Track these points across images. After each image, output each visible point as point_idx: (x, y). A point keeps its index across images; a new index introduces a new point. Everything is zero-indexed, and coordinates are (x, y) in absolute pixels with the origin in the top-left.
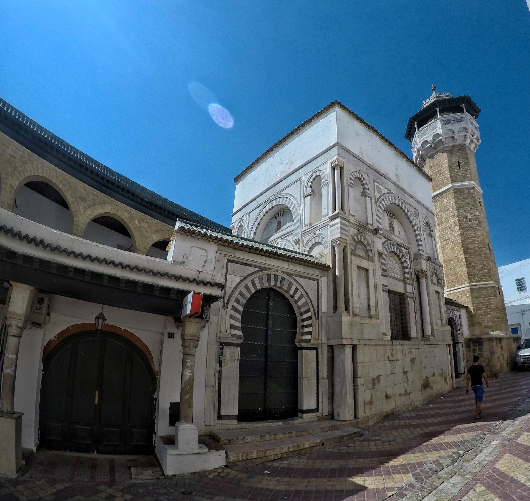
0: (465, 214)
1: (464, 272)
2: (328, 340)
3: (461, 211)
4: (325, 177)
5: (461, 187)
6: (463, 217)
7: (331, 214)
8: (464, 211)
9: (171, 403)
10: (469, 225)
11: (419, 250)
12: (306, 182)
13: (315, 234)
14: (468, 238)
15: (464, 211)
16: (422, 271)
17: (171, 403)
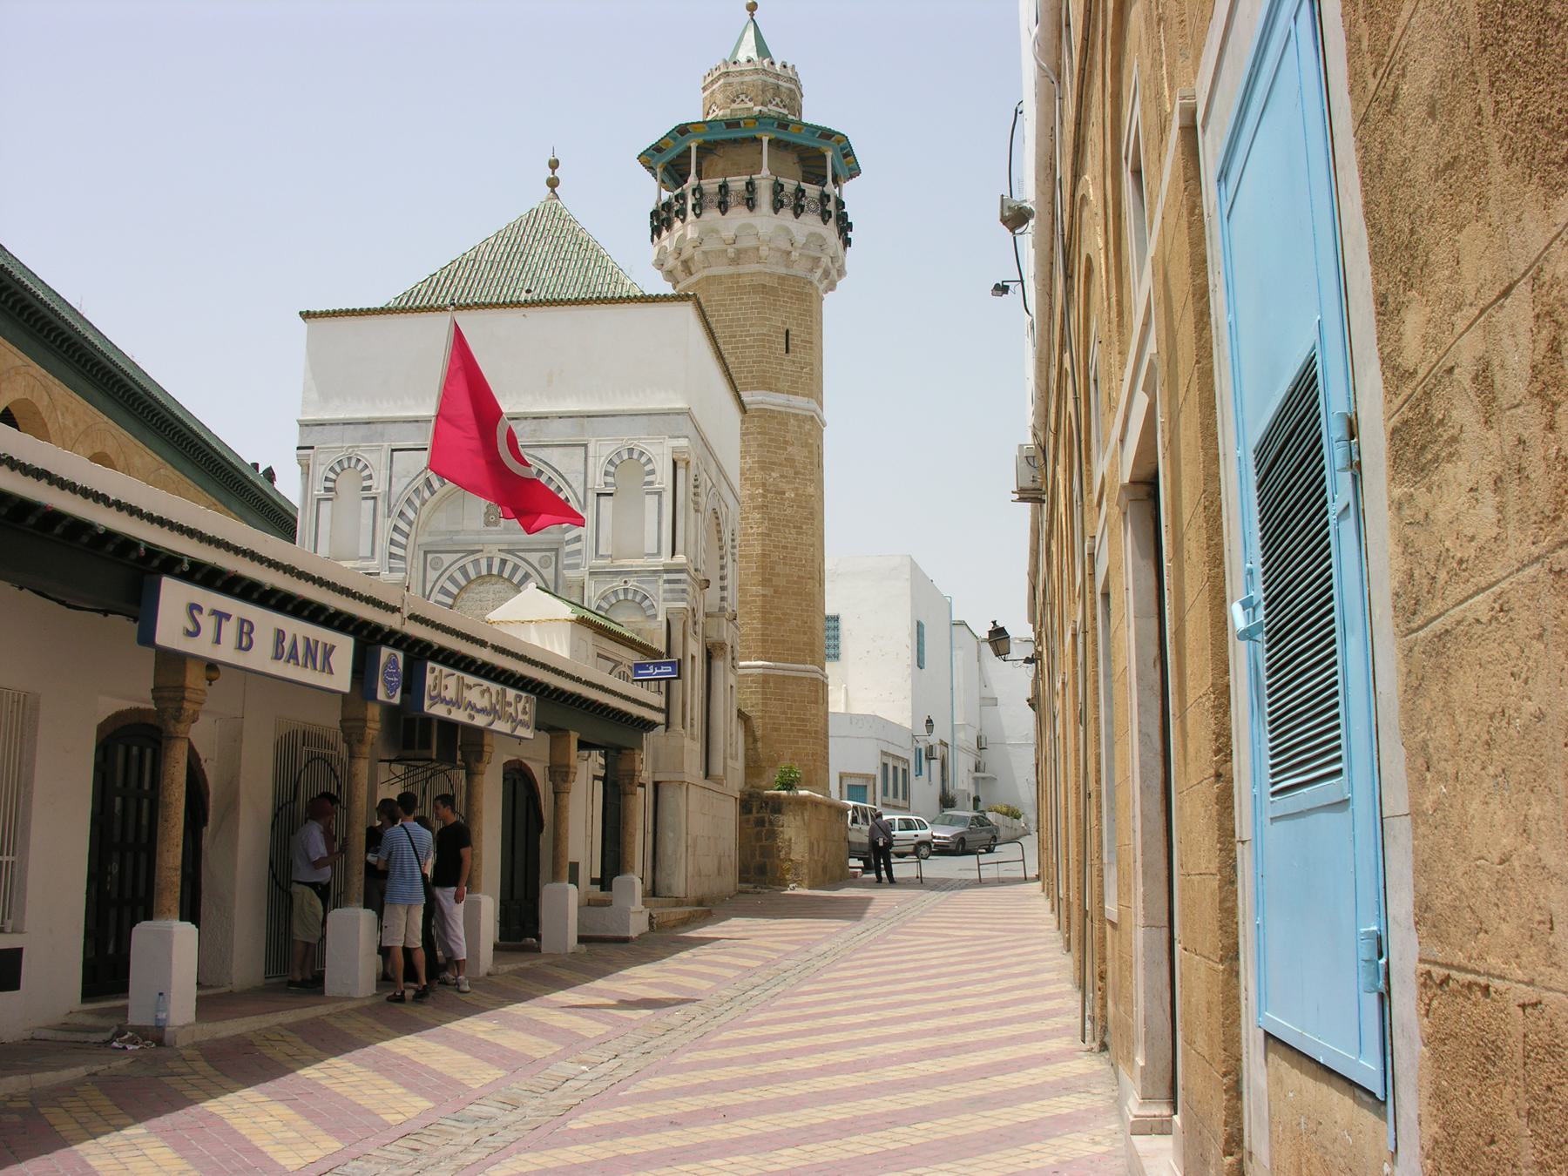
0: (783, 485)
1: (753, 629)
2: (654, 772)
3: (773, 474)
4: (652, 472)
5: (783, 409)
6: (776, 492)
7: (665, 559)
8: (781, 476)
9: (17, 987)
10: (786, 515)
11: (723, 599)
12: (603, 459)
13: (625, 582)
14: (778, 547)
15: (781, 476)
16: (722, 646)
17: (17, 987)
